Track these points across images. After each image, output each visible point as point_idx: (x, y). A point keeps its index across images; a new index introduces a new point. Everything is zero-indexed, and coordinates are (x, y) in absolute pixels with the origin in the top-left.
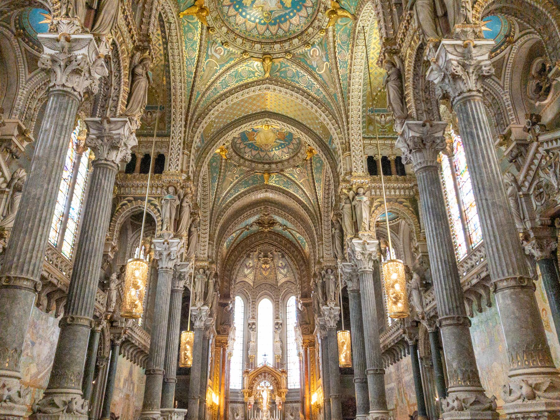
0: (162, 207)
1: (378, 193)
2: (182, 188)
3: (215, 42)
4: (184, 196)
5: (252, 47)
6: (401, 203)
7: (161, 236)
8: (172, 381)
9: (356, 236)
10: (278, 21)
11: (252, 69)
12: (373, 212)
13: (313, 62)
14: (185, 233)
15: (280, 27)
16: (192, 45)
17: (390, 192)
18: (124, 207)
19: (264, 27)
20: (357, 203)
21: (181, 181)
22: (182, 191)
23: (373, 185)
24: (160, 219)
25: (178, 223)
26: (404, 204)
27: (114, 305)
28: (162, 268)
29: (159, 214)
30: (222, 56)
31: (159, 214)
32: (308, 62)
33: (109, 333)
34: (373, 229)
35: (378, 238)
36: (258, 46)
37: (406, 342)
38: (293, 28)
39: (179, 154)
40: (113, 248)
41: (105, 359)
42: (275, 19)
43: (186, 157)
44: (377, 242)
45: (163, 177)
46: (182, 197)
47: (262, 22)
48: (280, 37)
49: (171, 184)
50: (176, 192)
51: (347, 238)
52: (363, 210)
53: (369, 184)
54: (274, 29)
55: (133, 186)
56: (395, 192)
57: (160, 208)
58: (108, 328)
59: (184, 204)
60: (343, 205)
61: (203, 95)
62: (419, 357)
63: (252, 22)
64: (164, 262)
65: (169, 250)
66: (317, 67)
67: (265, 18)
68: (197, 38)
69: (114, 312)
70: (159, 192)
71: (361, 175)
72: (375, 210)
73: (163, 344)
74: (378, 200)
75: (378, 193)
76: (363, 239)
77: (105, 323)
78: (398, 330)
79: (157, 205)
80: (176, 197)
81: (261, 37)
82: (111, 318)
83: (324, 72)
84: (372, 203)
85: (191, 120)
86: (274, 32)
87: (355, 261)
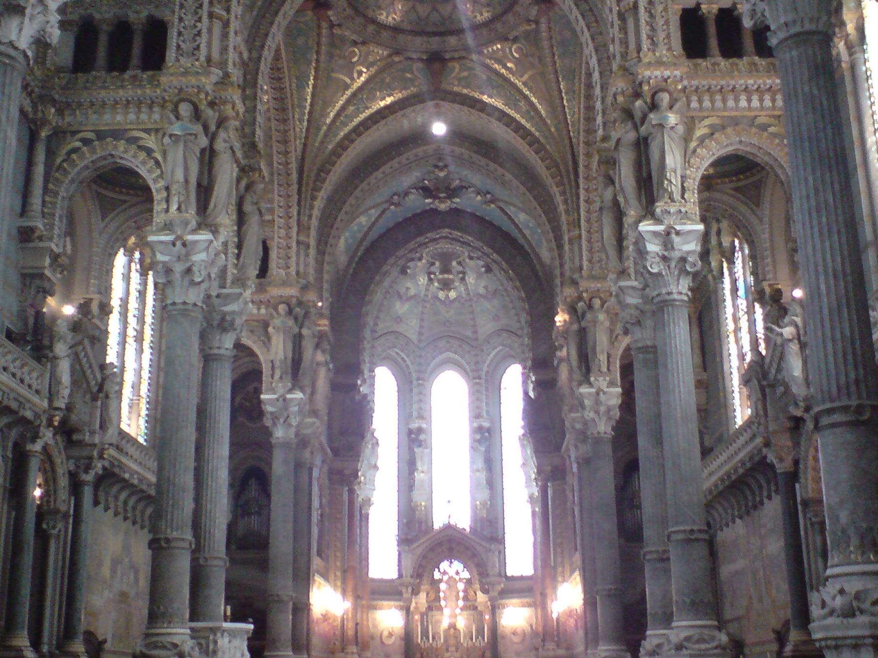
0: (164, 153)
1: (707, 104)
2: (212, 104)
4: (221, 122)
6: (764, 128)
7: (168, 227)
8: (216, 562)
9: (649, 212)
12: (694, 151)
14: (226, 221)
18: (74, 156)
20: (651, 130)
21: (209, 88)
22: (210, 112)
23: (695, 83)
24: (161, 184)
25: (204, 191)
26: (772, 129)
27: (66, 392)
28: (174, 304)
29: (158, 172)
31: (158, 172)
33: (64, 456)
34: (693, 197)
35: (703, 219)
37: (772, 466)
39: (200, 18)
40: (55, 257)
41: (59, 517)
43: (217, 26)
44: (701, 227)
45: (164, 79)
46: (213, 128)
49: (183, 96)
50: (197, 115)
51: (628, 220)
52: (667, 147)
53: (685, 82)
55: (92, 104)
56: (749, 101)
57: (160, 158)
58: (61, 446)
59: (219, 145)
62: (799, 499)
64: (178, 290)
65: (188, 260)
69: (69, 408)
71: (665, 59)
72: (698, 146)
73: (187, 479)
74: (707, 122)
75: (707, 104)
76: (666, 222)
77: (47, 436)
78: (753, 437)
79: (154, 151)
80: (198, 128)
82: (64, 422)
87: (647, 276)
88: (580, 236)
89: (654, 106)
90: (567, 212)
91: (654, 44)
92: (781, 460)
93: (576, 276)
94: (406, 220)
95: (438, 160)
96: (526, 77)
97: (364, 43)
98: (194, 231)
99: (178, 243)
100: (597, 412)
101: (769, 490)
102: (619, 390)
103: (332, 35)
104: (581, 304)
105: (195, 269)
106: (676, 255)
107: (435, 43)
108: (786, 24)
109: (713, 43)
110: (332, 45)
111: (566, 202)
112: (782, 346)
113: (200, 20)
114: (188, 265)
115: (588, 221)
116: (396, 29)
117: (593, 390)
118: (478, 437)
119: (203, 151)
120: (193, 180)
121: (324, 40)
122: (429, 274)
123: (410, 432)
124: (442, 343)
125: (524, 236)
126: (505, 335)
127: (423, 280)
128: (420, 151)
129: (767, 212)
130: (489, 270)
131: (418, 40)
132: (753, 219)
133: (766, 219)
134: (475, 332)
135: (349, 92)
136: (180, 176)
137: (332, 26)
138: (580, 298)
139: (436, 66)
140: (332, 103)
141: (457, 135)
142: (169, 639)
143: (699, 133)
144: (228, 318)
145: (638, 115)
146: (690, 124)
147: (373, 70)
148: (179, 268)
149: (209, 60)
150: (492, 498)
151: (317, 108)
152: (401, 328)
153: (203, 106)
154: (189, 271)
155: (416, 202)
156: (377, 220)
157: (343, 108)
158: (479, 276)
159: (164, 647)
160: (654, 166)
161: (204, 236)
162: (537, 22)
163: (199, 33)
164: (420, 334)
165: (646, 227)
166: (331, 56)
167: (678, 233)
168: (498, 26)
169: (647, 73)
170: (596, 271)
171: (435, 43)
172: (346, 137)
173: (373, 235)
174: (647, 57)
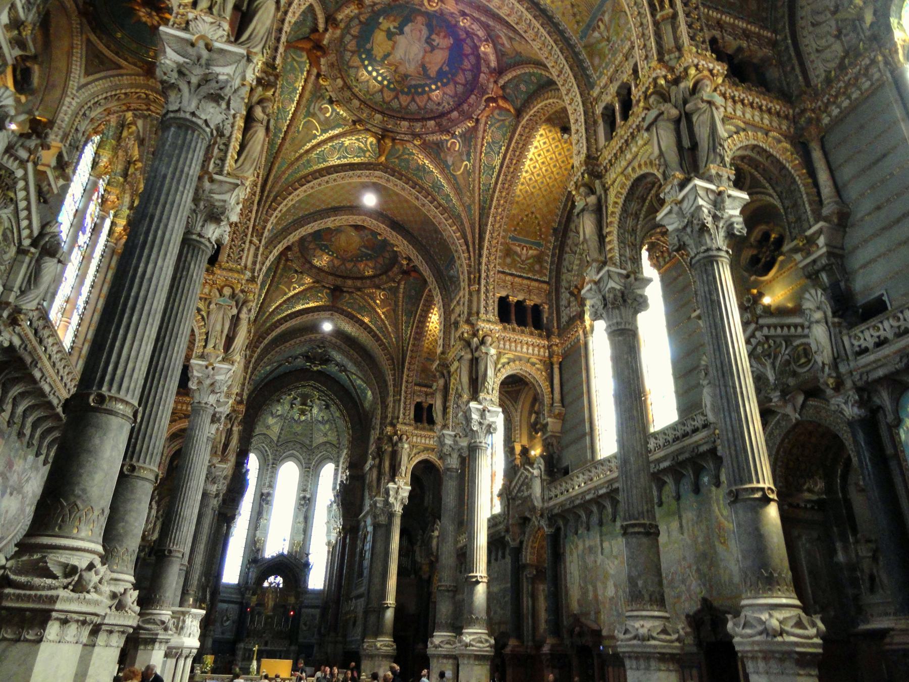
0: (208, 313)
1: (507, 346)
2: (242, 291)
3: (322, 97)
4: (245, 302)
5: (370, 117)
6: (533, 364)
9: (475, 397)
10: (413, 90)
11: (362, 146)
12: (499, 370)
13: (448, 158)
15: (413, 100)
16: (290, 93)
17: (522, 348)
19: (392, 94)
22: (241, 295)
24: (204, 330)
26: (537, 366)
30: (327, 118)
32: (442, 155)
36: (378, 117)
38: (430, 105)
42: (409, 88)
47: (392, 86)
48: (412, 114)
49: (228, 283)
54: (404, 100)
60: (463, 354)
61: (292, 164)
63: (379, 82)
66: (453, 164)
67: (397, 81)
68: (300, 85)
70: (206, 290)
74: (507, 356)
75: (507, 346)
81: (385, 106)
83: (462, 174)
84: (499, 358)
85: (268, 196)
86: (404, 104)
88: (400, 400)
89: (483, 342)
90: (394, 385)
91: (487, 312)
92: (514, 540)
93: (395, 421)
94: (290, 372)
95: (323, 341)
96: (384, 310)
97: (301, 273)
98: (220, 362)
99: (210, 368)
100: (396, 499)
101: (497, 555)
102: (410, 488)
103: (285, 265)
104: (395, 437)
105: (217, 385)
106: (486, 422)
107: (339, 282)
108: (617, 323)
109: (513, 317)
110: (284, 269)
111: (394, 380)
112: (531, 479)
113: (244, 243)
114: (212, 381)
115: (406, 392)
116: (320, 269)
117: (396, 486)
118: (303, 502)
119: (233, 316)
120: (225, 332)
121: (281, 266)
122: (292, 404)
123: (262, 494)
124: (290, 445)
125: (357, 393)
126: (328, 445)
127: (287, 407)
128: (313, 336)
129: (520, 406)
130: (327, 407)
131: (330, 278)
132: (512, 408)
133: (519, 410)
134: (311, 442)
135: (285, 297)
136: (218, 327)
137: (287, 260)
138: (396, 434)
139: (338, 293)
140: (275, 301)
141: (338, 333)
142: (159, 618)
143: (504, 360)
144: (218, 415)
145: (474, 346)
146: (499, 355)
147: (302, 288)
148: (208, 382)
149: (246, 267)
150: (304, 540)
151: (266, 302)
152: (268, 432)
153: (237, 291)
154: (212, 384)
155: (300, 362)
156: (276, 369)
157: (281, 305)
158: (320, 410)
159: (155, 623)
160: (481, 373)
161: (225, 366)
162: (399, 283)
163: (243, 250)
164: (279, 437)
165: (473, 405)
166: (282, 275)
167: (489, 411)
168: (377, 280)
169: (483, 325)
170: (407, 421)
171: (339, 282)
172: (278, 321)
173: (271, 377)
174: (483, 316)
